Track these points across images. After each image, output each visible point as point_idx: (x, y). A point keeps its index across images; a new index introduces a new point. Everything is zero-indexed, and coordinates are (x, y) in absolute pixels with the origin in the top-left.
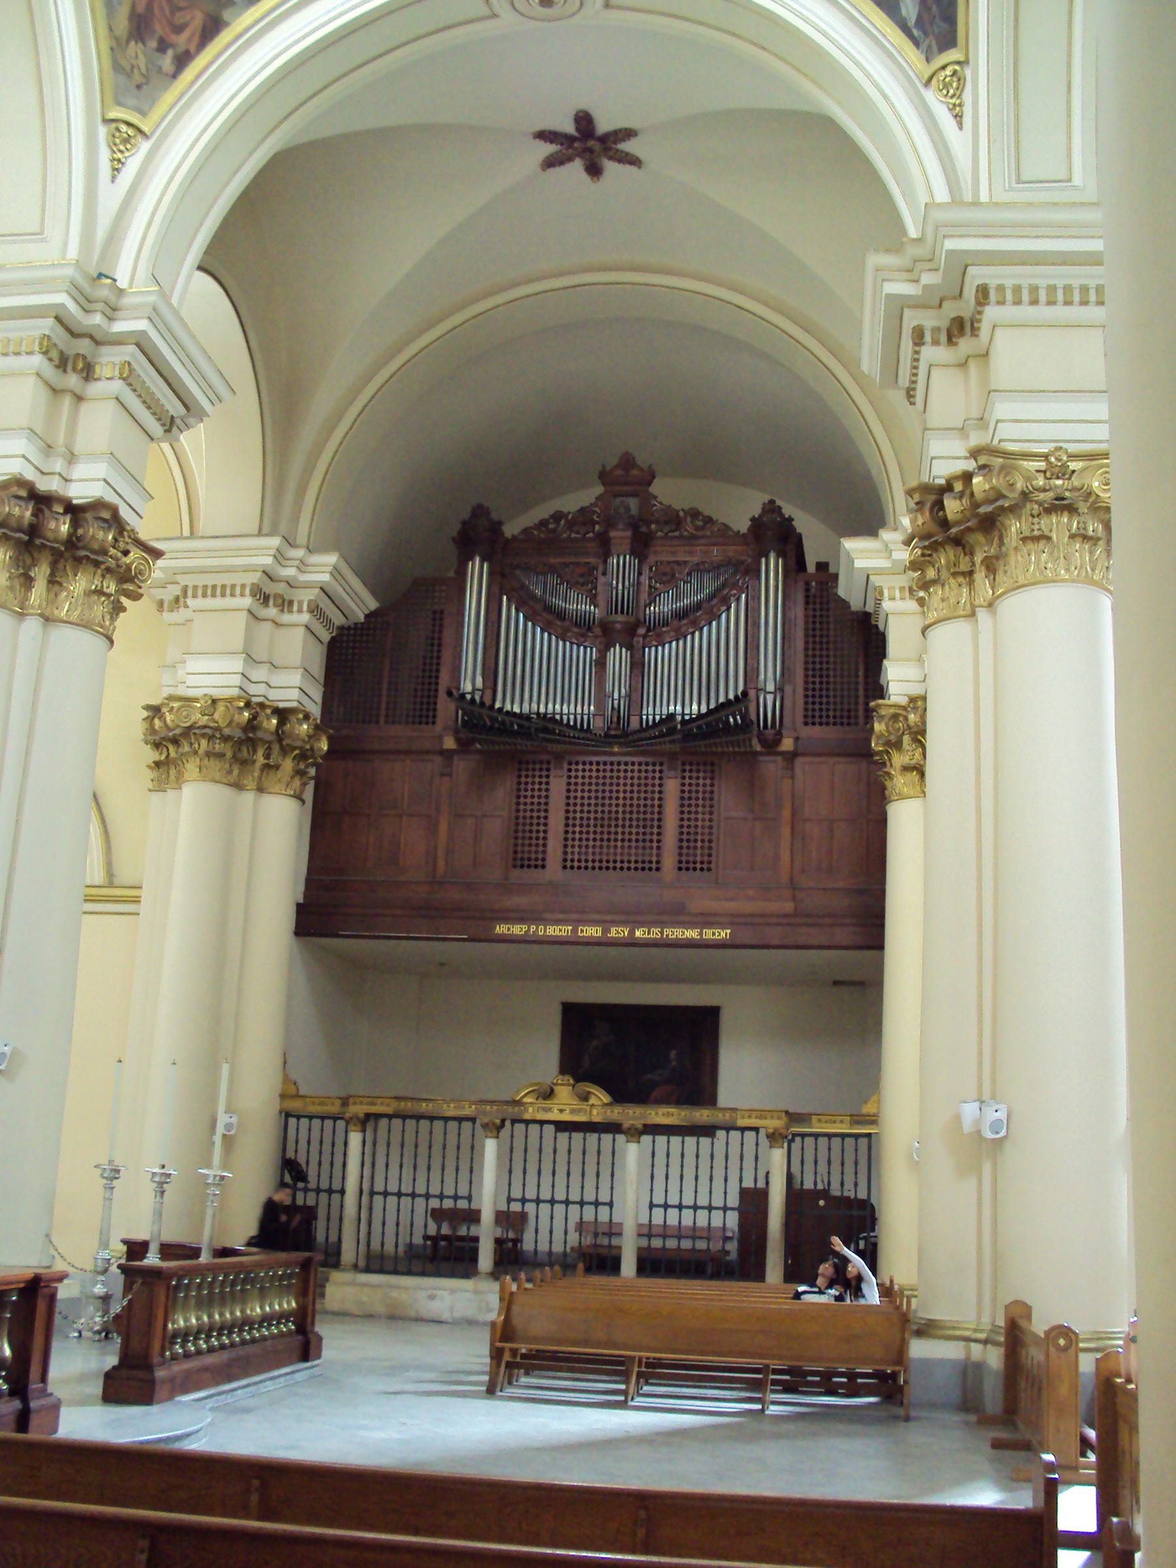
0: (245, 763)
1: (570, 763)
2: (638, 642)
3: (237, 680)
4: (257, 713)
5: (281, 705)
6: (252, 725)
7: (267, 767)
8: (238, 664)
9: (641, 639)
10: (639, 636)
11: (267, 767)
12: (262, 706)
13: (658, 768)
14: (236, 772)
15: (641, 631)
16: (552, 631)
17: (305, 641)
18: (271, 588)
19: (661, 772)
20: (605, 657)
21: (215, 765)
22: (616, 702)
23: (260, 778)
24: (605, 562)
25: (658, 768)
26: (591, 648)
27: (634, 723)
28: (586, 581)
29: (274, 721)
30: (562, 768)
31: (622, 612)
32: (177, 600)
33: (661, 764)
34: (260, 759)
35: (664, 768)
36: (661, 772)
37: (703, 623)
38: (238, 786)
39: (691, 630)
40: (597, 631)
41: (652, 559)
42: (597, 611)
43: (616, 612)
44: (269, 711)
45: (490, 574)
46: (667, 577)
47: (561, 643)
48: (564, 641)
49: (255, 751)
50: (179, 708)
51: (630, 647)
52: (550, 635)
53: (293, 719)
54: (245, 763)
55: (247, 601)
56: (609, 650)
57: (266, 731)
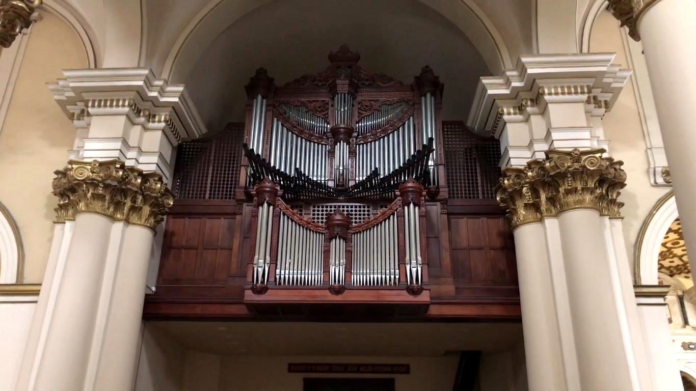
0: (118, 206)
1: (314, 207)
2: (353, 141)
3: (116, 154)
4: (129, 174)
5: (144, 173)
6: (123, 180)
7: (133, 209)
8: (118, 145)
9: (355, 139)
10: (354, 137)
11: (133, 209)
12: (132, 169)
13: (366, 209)
14: (111, 209)
15: (355, 134)
16: (303, 136)
17: (161, 141)
18: (142, 105)
19: (368, 211)
20: (335, 149)
21: (98, 205)
22: (341, 171)
23: (128, 215)
24: (333, 99)
25: (366, 209)
26: (326, 145)
27: (352, 183)
28: (322, 111)
29: (139, 181)
30: (310, 210)
31: (344, 123)
32: (83, 111)
33: (368, 207)
34: (129, 203)
35: (370, 209)
36: (368, 211)
37: (389, 131)
38: (113, 218)
39: (383, 135)
40: (329, 135)
41: (359, 99)
42: (328, 126)
43: (341, 122)
44: (136, 174)
45: (267, 106)
46: (367, 110)
47: (308, 143)
48: (310, 142)
49: (126, 198)
50: (77, 169)
51: (348, 143)
52: (302, 138)
53: (151, 180)
54: (118, 206)
55: (127, 109)
56: (337, 145)
57: (134, 185)
